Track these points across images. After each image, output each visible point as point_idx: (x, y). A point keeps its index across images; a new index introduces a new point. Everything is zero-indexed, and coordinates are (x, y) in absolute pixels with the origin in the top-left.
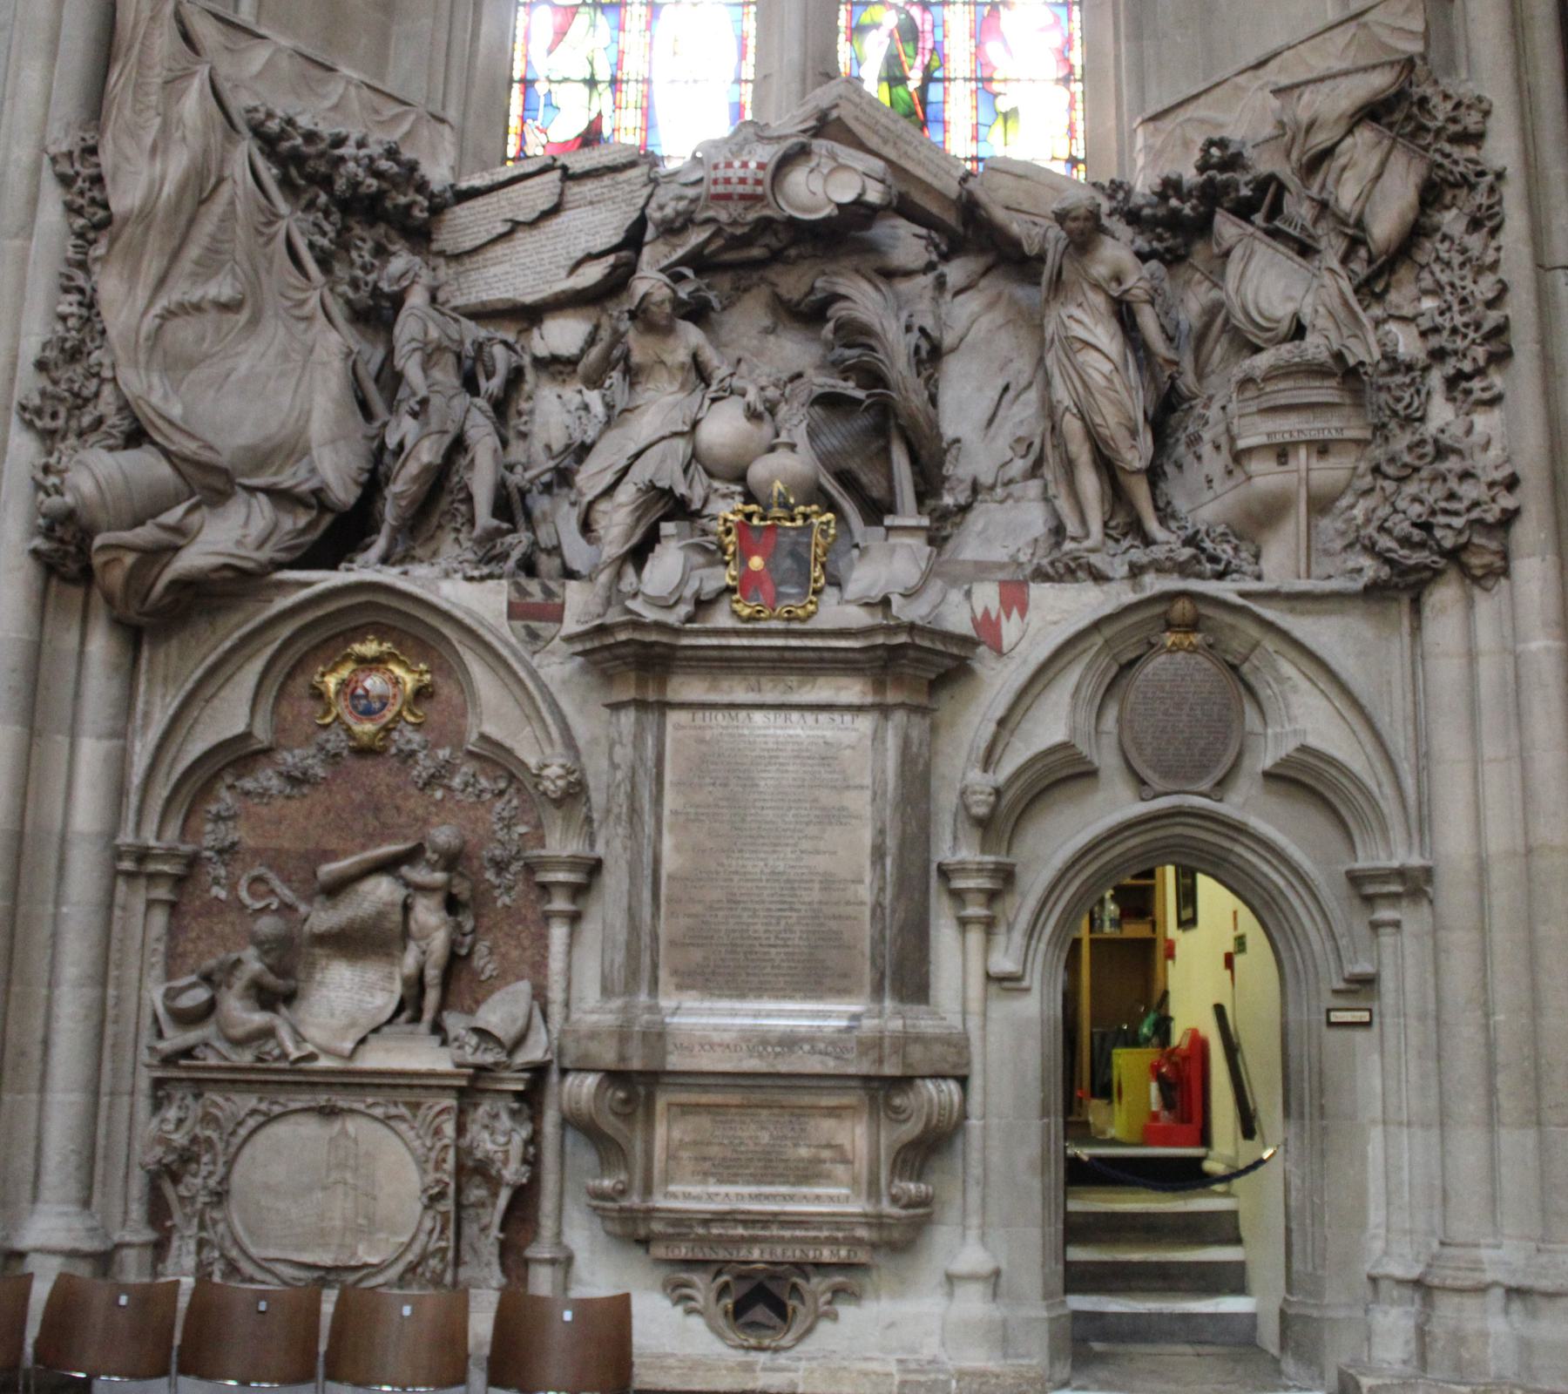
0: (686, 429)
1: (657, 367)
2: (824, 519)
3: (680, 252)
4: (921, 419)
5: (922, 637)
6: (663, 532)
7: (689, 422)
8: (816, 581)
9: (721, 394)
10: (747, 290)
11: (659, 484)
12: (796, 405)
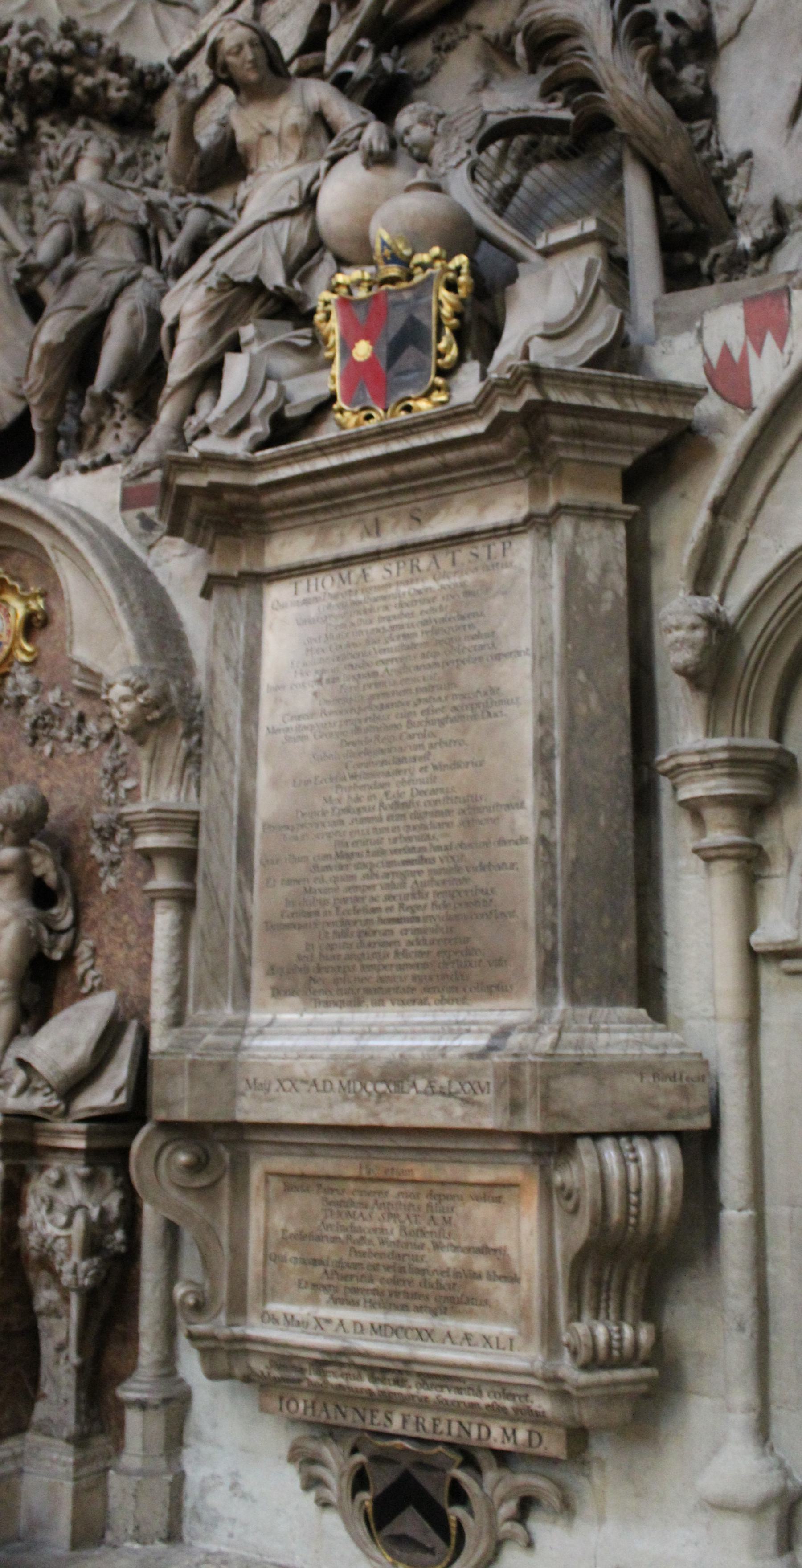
0: (295, 204)
1: (265, 141)
2: (452, 265)
3: (357, 22)
4: (638, 112)
5: (566, 389)
6: (243, 340)
7: (296, 195)
8: (440, 355)
9: (343, 149)
10: (450, 48)
11: (237, 279)
12: (455, 140)
